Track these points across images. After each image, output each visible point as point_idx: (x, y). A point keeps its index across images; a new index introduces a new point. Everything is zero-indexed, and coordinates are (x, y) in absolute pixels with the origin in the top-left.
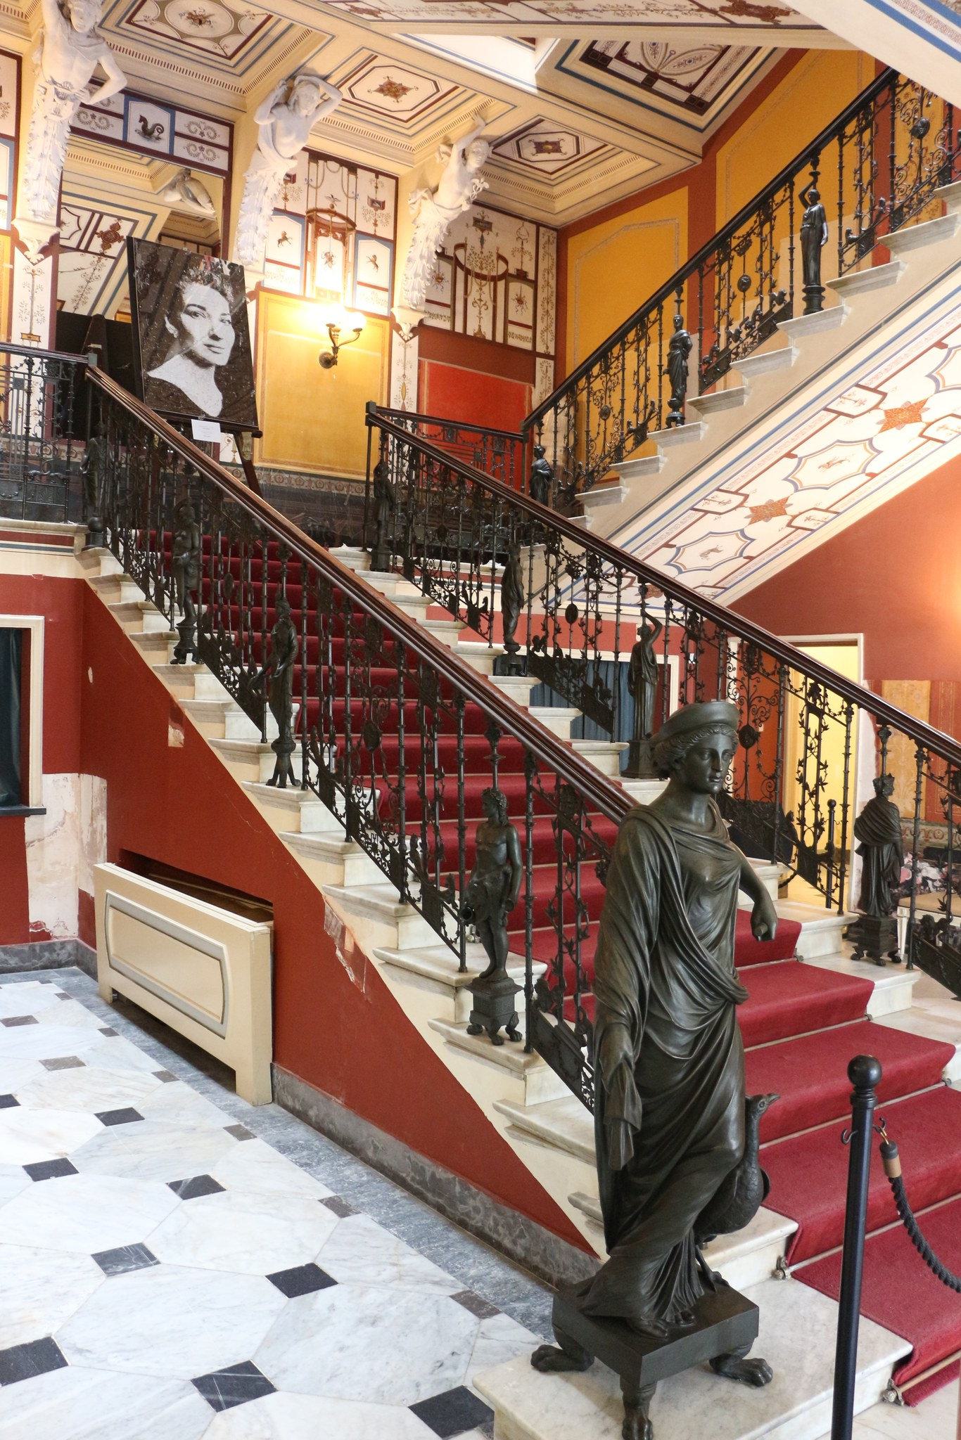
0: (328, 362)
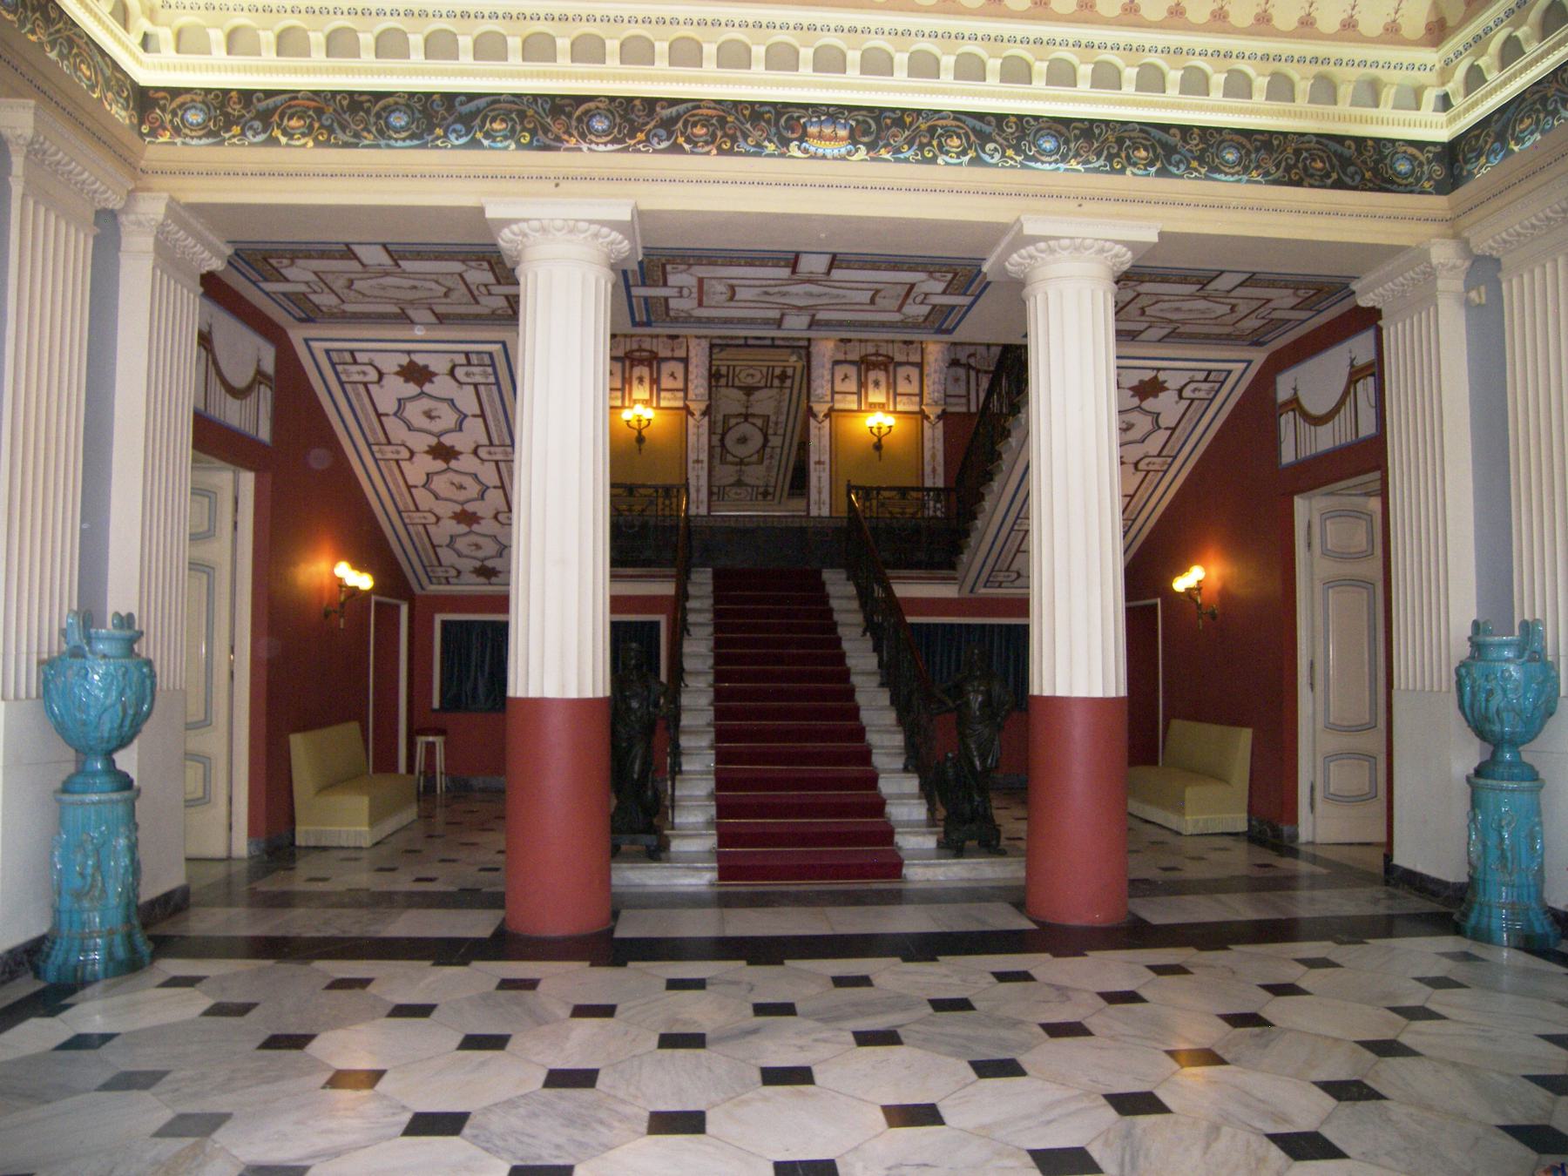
0: (878, 446)
